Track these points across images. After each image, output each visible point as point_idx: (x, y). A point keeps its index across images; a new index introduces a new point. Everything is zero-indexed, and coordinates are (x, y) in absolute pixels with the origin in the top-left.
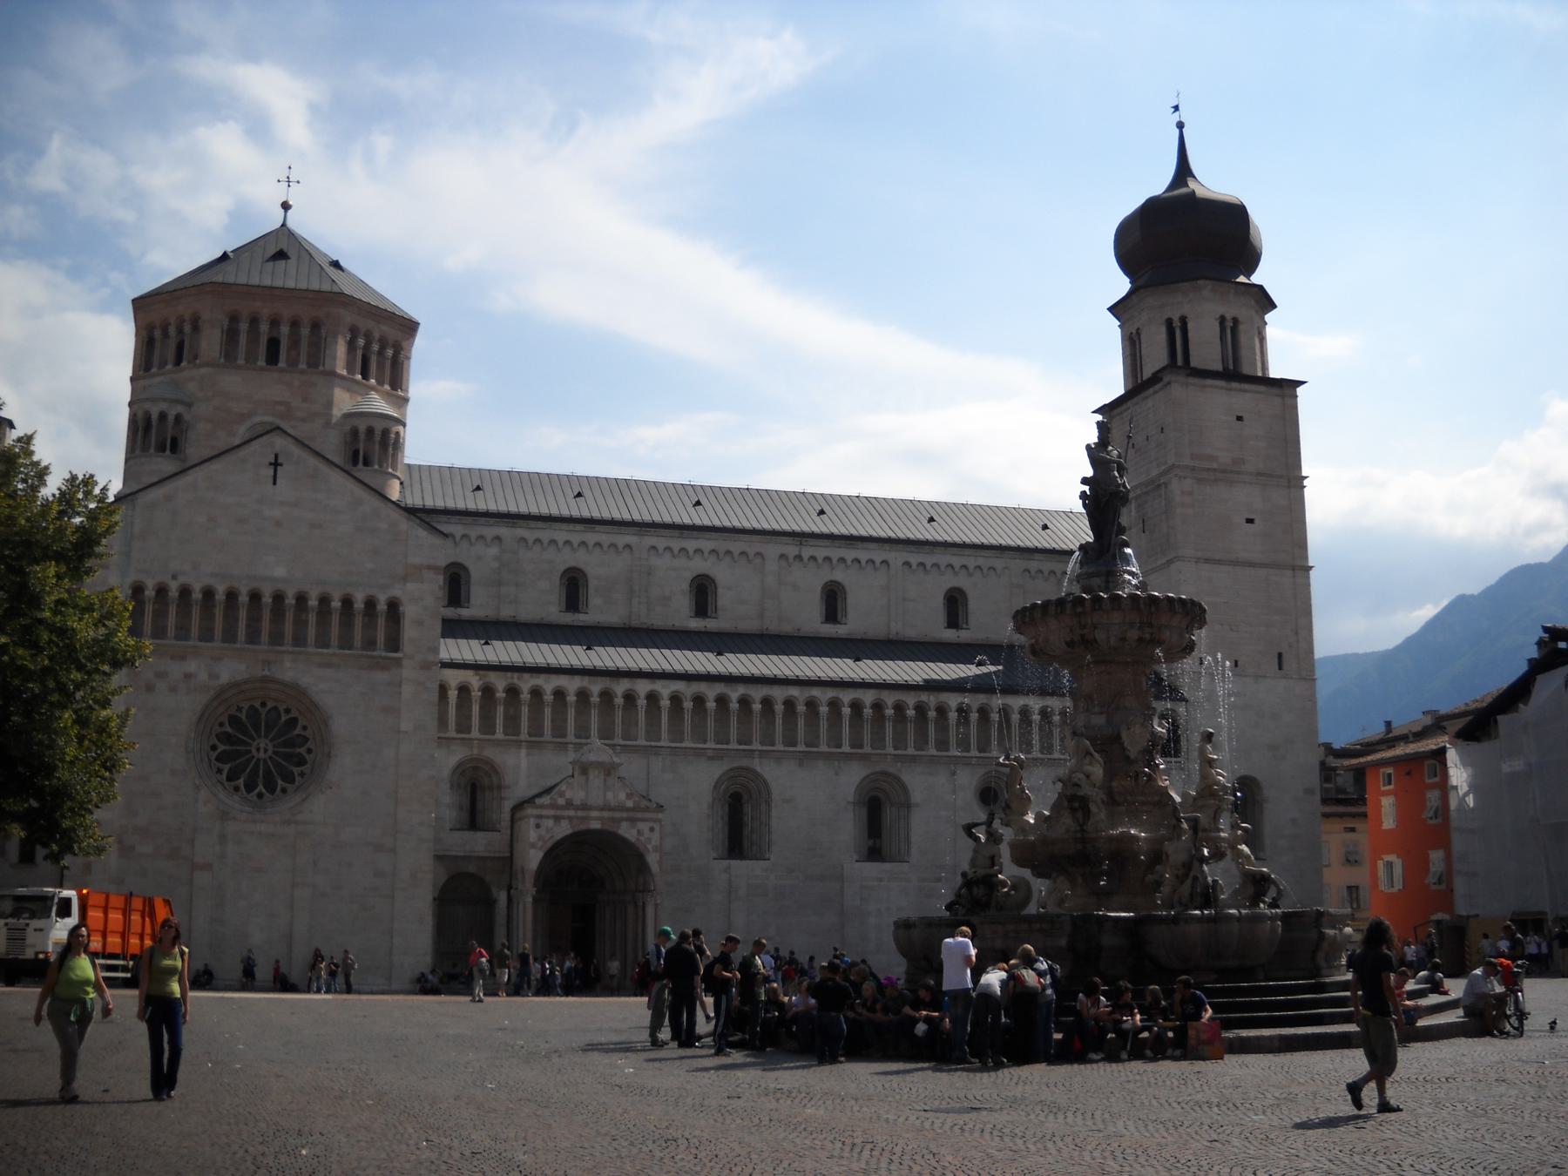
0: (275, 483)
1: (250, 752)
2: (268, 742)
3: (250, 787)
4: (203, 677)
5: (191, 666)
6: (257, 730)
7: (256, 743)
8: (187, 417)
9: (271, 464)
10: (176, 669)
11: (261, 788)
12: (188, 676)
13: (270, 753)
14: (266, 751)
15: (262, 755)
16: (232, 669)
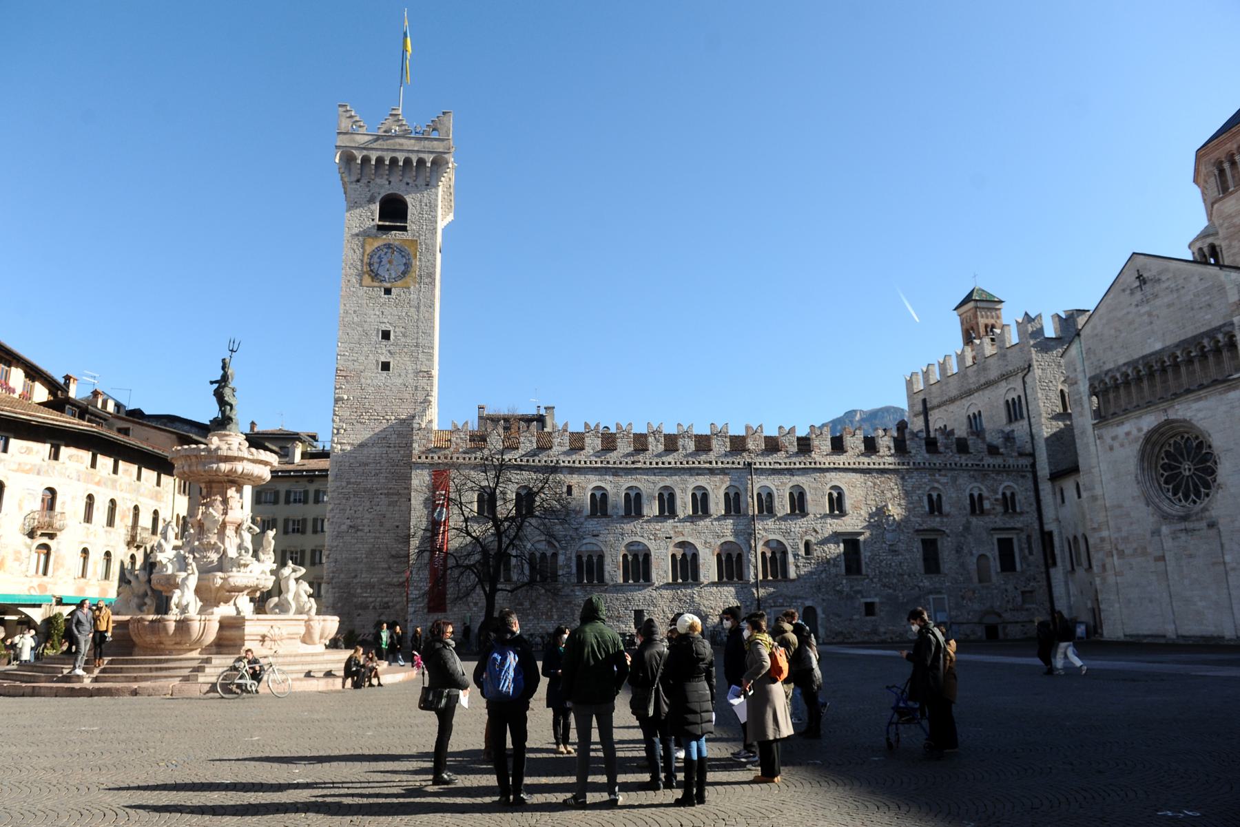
0: (1142, 290)
1: (1181, 473)
2: (1189, 463)
3: (1186, 497)
4: (1135, 432)
5: (1127, 427)
6: (1183, 457)
7: (1182, 466)
8: (1217, 243)
9: (1137, 278)
10: (1121, 431)
11: (1193, 496)
12: (1128, 434)
13: (1192, 470)
14: (1190, 470)
15: (1187, 473)
16: (1149, 421)
